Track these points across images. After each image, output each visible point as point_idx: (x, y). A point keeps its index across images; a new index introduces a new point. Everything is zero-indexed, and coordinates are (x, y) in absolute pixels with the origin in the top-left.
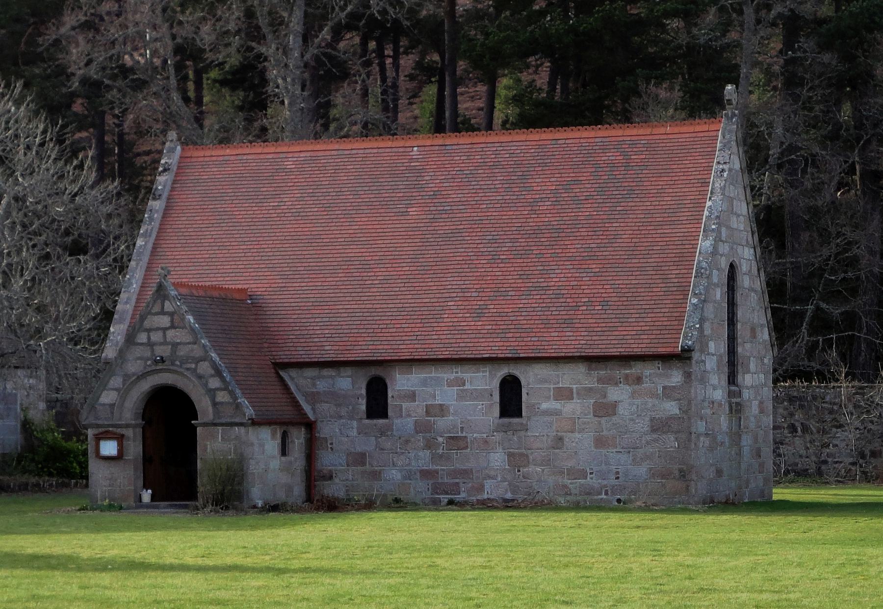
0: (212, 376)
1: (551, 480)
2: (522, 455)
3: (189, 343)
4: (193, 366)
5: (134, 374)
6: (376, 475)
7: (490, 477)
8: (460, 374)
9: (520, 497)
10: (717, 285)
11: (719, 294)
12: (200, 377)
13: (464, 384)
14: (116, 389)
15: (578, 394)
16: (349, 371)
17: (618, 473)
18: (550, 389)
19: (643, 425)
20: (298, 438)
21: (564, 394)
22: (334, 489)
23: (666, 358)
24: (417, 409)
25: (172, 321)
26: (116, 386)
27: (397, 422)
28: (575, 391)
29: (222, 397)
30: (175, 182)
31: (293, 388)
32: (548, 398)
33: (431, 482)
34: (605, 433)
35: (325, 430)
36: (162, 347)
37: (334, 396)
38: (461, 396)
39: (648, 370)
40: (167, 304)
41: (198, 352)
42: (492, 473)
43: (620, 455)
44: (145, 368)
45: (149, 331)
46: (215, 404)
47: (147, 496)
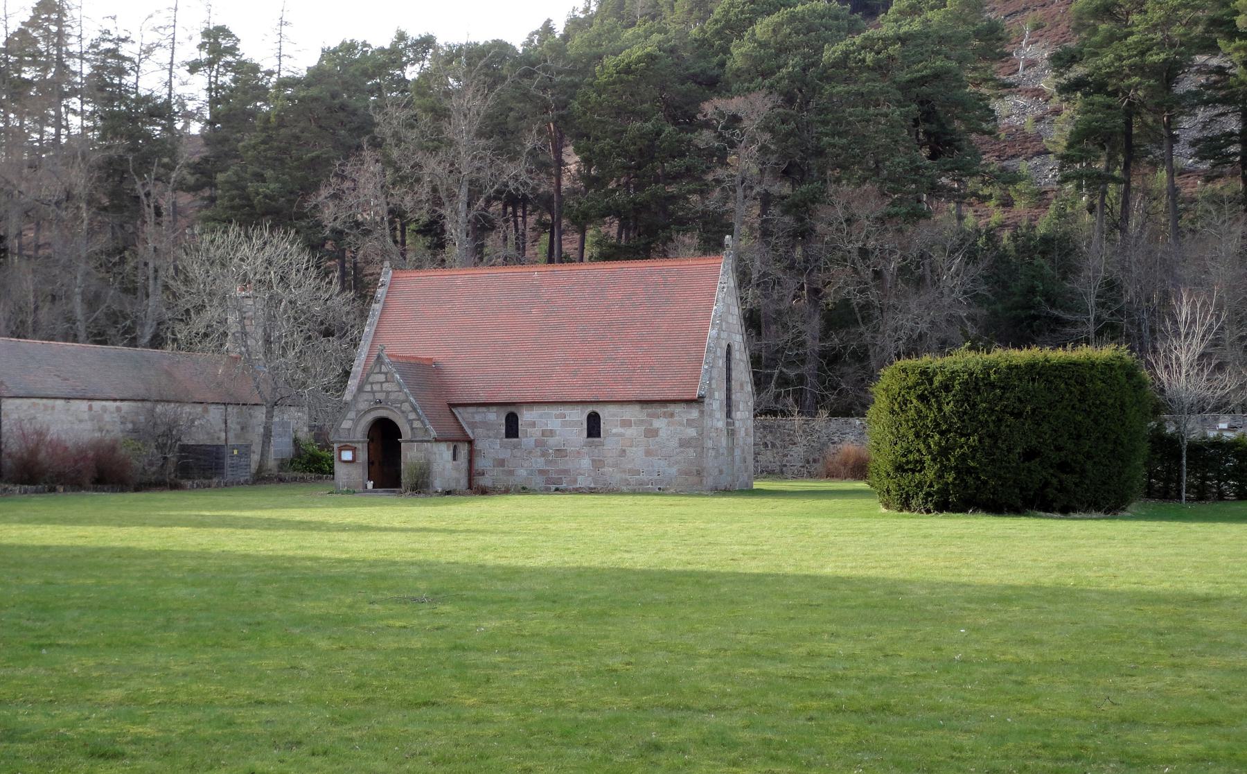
1: (618, 476)
6: (511, 473)
9: (599, 486)
10: (719, 357)
11: (721, 363)
12: (403, 412)
16: (495, 409)
19: (674, 443)
20: (463, 450)
21: (626, 424)
22: (485, 481)
23: (689, 402)
24: (535, 433)
27: (524, 440)
29: (417, 424)
30: (388, 292)
31: (460, 419)
35: (479, 445)
37: (485, 424)
38: (564, 424)
39: (677, 409)
40: (383, 367)
41: (401, 397)
42: (582, 472)
45: (372, 384)
46: (412, 429)
47: (370, 485)
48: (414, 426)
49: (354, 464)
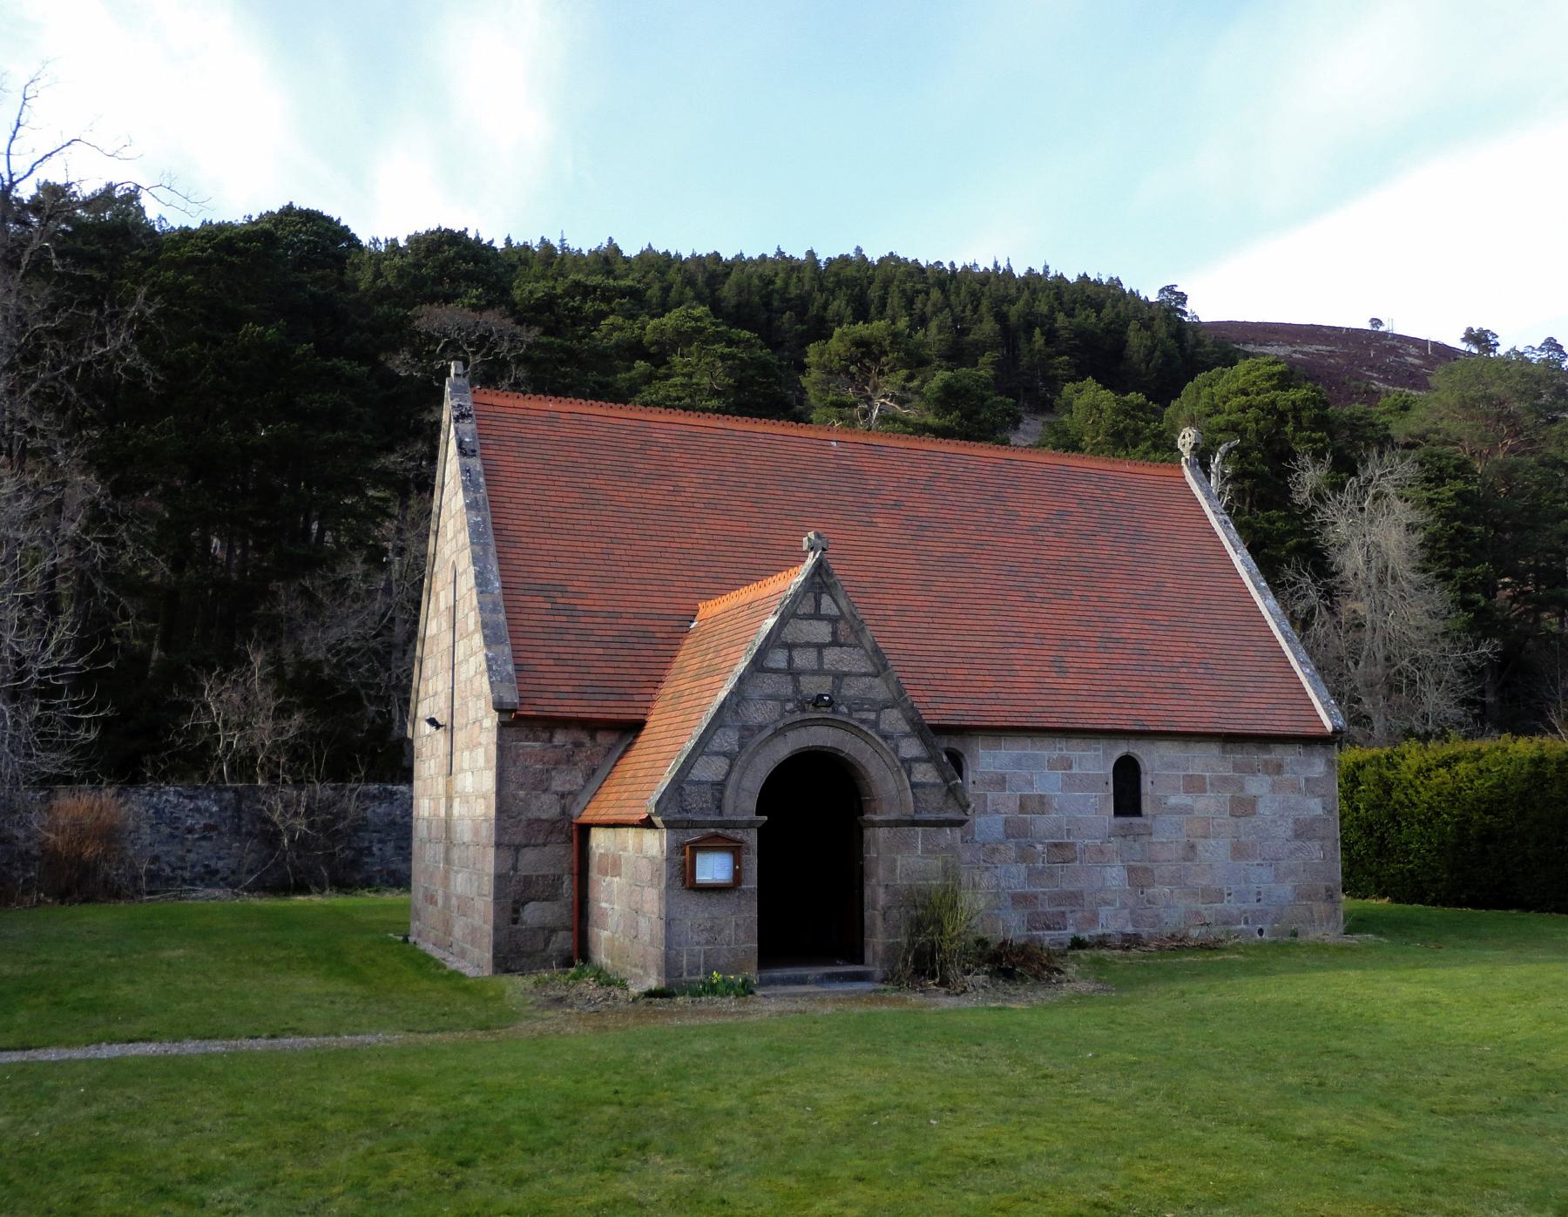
0: (907, 735)
2: (1146, 870)
3: (865, 675)
4: (872, 716)
5: (761, 728)
7: (1107, 903)
8: (1065, 752)
13: (1070, 767)
14: (724, 754)
15: (1212, 785)
17: (1259, 893)
18: (1178, 776)
19: (1285, 829)
21: (1194, 785)
24: (1006, 801)
25: (834, 633)
26: (727, 748)
28: (1208, 781)
32: (1177, 789)
33: (1026, 912)
34: (1243, 839)
36: (816, 679)
38: (1070, 783)
39: (1288, 756)
40: (826, 600)
42: (1109, 897)
43: (1261, 869)
44: (782, 716)
45: (790, 647)
46: (914, 786)
48: (918, 777)
49: (733, 896)
